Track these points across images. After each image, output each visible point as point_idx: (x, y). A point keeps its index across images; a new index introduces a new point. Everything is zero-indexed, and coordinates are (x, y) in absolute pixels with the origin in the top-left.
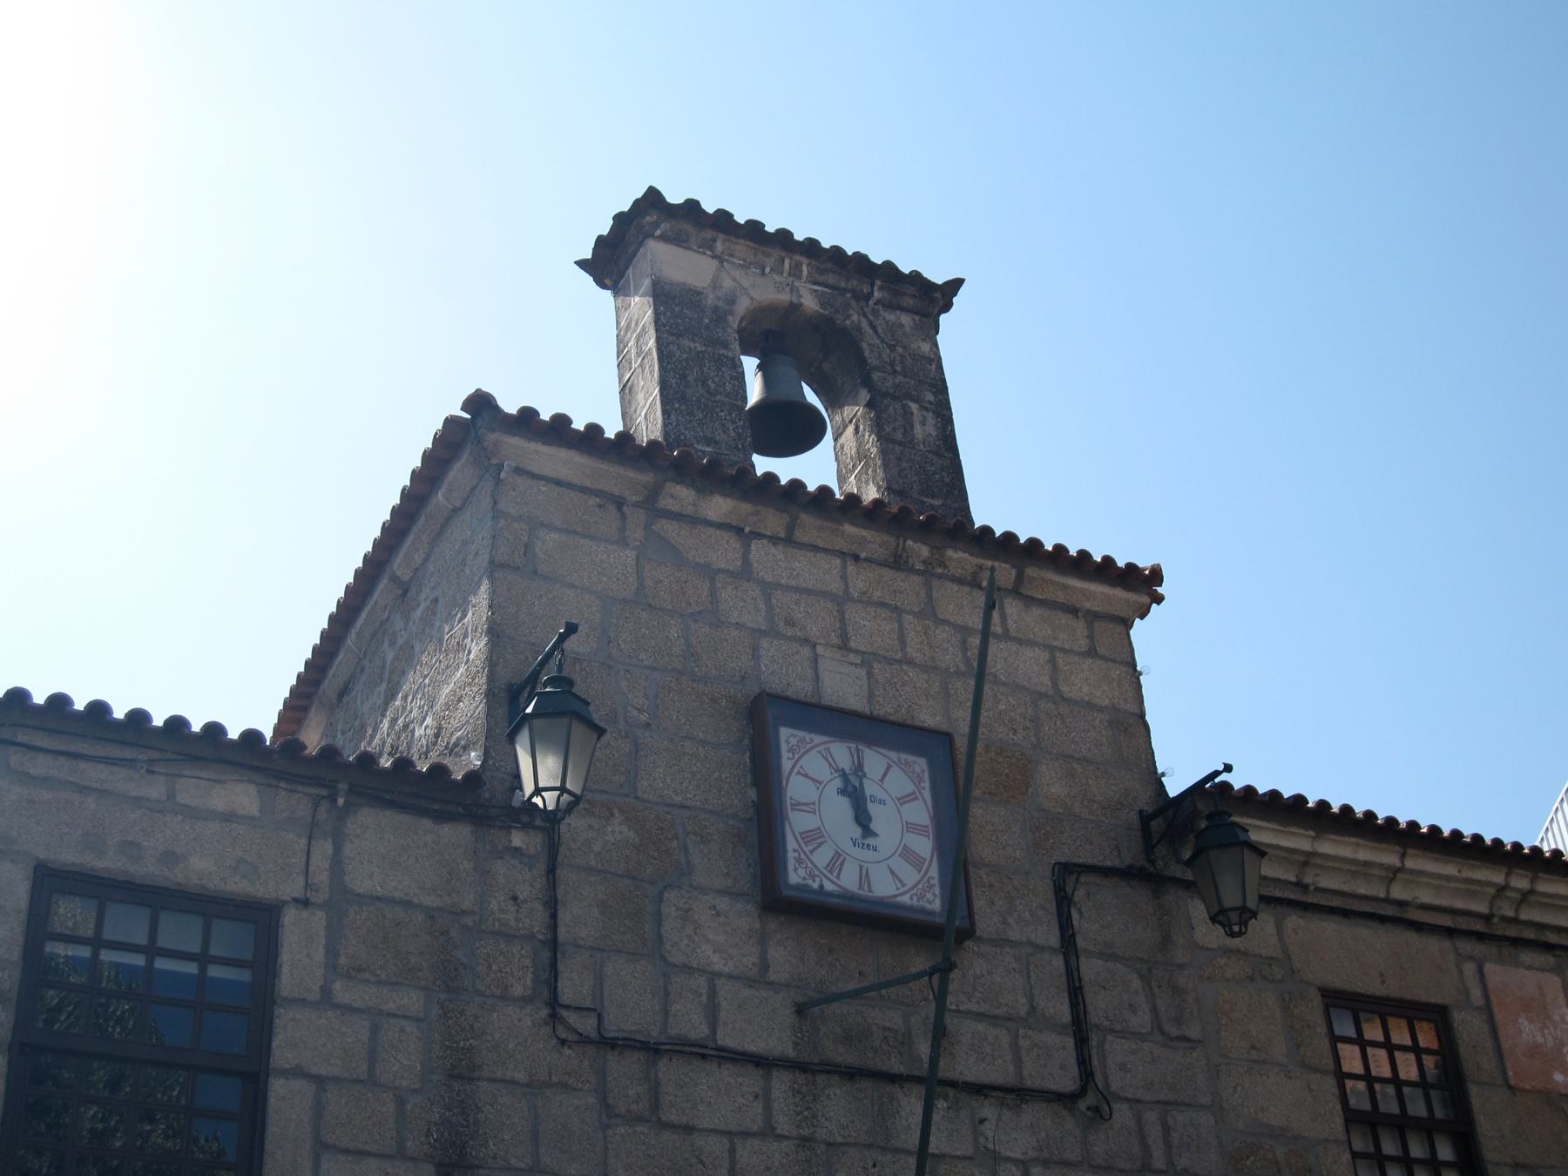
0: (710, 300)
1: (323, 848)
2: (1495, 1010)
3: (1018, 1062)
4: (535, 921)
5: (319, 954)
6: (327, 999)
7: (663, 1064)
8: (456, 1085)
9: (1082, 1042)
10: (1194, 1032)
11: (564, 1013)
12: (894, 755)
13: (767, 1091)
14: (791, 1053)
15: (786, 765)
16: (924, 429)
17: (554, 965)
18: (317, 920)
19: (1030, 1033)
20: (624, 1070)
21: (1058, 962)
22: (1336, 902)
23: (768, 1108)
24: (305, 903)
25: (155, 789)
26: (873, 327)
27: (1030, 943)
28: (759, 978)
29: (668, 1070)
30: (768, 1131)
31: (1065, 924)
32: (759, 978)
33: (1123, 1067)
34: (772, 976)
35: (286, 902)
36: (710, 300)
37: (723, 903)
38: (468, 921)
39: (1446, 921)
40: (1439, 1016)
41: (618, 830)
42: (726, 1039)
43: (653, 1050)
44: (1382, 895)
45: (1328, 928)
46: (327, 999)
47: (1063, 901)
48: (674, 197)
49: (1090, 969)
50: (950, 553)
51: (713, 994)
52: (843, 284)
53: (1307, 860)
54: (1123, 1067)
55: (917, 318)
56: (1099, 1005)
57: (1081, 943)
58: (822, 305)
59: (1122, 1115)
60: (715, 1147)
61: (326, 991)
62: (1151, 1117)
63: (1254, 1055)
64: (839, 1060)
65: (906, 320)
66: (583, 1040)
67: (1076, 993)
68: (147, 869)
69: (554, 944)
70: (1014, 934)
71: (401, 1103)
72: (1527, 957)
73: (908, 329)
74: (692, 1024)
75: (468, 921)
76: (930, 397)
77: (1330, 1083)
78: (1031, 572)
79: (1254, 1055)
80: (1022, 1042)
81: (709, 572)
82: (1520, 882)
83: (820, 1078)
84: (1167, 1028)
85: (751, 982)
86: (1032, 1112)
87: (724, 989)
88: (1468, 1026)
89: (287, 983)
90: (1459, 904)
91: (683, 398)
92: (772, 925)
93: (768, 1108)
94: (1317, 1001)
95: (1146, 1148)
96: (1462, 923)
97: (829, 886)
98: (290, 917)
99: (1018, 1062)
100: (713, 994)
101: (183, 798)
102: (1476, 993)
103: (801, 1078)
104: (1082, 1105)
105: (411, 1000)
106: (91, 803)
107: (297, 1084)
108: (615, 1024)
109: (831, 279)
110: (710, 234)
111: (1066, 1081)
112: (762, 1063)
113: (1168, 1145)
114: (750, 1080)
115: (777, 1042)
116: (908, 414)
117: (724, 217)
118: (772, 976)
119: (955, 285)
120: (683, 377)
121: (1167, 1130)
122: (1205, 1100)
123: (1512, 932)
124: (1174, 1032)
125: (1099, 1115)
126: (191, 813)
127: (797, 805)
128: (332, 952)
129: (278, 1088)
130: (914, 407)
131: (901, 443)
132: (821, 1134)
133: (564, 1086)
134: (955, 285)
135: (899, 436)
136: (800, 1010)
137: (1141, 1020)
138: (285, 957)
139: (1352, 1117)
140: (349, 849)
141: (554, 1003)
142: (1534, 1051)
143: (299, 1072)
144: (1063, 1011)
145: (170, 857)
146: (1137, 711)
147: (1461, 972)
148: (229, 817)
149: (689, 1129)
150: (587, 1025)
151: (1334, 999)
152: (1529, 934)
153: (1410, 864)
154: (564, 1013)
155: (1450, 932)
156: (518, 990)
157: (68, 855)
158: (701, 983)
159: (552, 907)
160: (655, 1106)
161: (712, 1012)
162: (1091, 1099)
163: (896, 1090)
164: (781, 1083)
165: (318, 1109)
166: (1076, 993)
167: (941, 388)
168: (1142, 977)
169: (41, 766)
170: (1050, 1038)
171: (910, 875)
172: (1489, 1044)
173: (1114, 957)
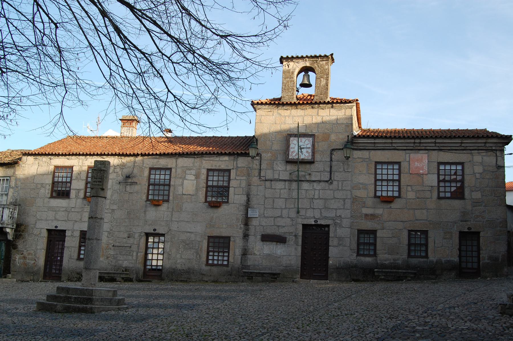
0: (291, 71)
1: (235, 162)
2: (411, 162)
3: (321, 177)
4: (258, 167)
5: (235, 174)
6: (235, 179)
7: (272, 182)
8: (249, 186)
9: (331, 174)
10: (350, 170)
11: (261, 177)
12: (307, 138)
13: (285, 184)
14: (289, 179)
15: (291, 143)
16: (323, 82)
17: (260, 172)
18: (234, 170)
19: (324, 174)
20: (268, 183)
21: (329, 163)
22: (382, 148)
23: (285, 186)
24: (233, 169)
25: (218, 159)
26: (318, 66)
27: (325, 161)
28: (286, 170)
29: (273, 182)
30: (285, 188)
31: (331, 158)
32: (286, 170)
33: (337, 176)
34: (287, 170)
35: (231, 169)
36: (291, 71)
37: (281, 162)
38: (251, 168)
39: (405, 148)
40: (399, 163)
41: (269, 154)
42: (280, 178)
43: (271, 181)
44: (391, 146)
45: (379, 152)
46: (235, 179)
47: (331, 154)
48: (285, 56)
49: (334, 163)
50: (321, 105)
51: (279, 173)
52: (314, 60)
53: (374, 143)
54: (337, 176)
55: (326, 61)
56: (334, 169)
57: (333, 160)
58: (310, 65)
59: (335, 183)
60: (278, 191)
61: (235, 178)
62: (340, 183)
63: (360, 173)
64: (295, 179)
65: (324, 62)
66: (263, 180)
67: (331, 167)
68: (217, 168)
69: (260, 169)
70: (323, 160)
71: (243, 189)
72: (421, 152)
73: (324, 64)
74: (276, 177)
75: (251, 168)
76: (325, 76)
77: (373, 176)
78: (334, 105)
79: (360, 173)
80: (322, 175)
81: (285, 116)
82: (417, 141)
83: (292, 182)
84: (345, 170)
85: (284, 171)
86: (322, 184)
87: (281, 172)
88: (404, 165)
89: (231, 178)
90: (407, 145)
91: (285, 90)
92: (288, 164)
93: (285, 186)
94: (374, 163)
95: (338, 186)
96: (408, 148)
97: (295, 158)
98: (232, 171)
99: (321, 177)
100: (279, 173)
101: (221, 160)
102: (408, 159)
103: (290, 182)
104: (329, 182)
105: (244, 178)
106: (212, 162)
107: (233, 188)
108: (267, 178)
109: (311, 60)
110: (292, 59)
111: (328, 179)
112: (285, 181)
113: (342, 186)
114: (283, 183)
115: (287, 178)
116: (321, 81)
117: (292, 57)
118: (287, 170)
119: (332, 55)
120: (285, 86)
121: (342, 184)
122: (350, 180)
123: (419, 148)
124: (346, 171)
125: (331, 183)
126: (222, 161)
127: (292, 148)
128: (236, 174)
129: (230, 188)
130: (322, 79)
131: (318, 87)
132: (291, 188)
133: (261, 185)
134: (332, 55)
135: (318, 86)
136: (290, 174)
137: (342, 170)
138: (231, 175)
139: (376, 180)
140: (238, 162)
141: (260, 176)
142: (417, 167)
143: (233, 187)
144: (329, 170)
145: (220, 166)
146: (350, 122)
147: (406, 156)
148: (225, 161)
149: (275, 189)
150: (264, 178)
151: (377, 163)
152: (424, 148)
153: (393, 141)
154: (261, 177)
155: (405, 150)
156: (256, 175)
157: (210, 168)
158: (278, 172)
159: (260, 165)
160: (271, 187)
161: (279, 175)
162: (331, 181)
163: (303, 182)
164: (287, 183)
165: (234, 191)
166: (331, 167)
167: (328, 74)
168: (343, 163)
169: (207, 159)
170: (326, 173)
171: (307, 155)
172: (408, 167)
173: (339, 161)
